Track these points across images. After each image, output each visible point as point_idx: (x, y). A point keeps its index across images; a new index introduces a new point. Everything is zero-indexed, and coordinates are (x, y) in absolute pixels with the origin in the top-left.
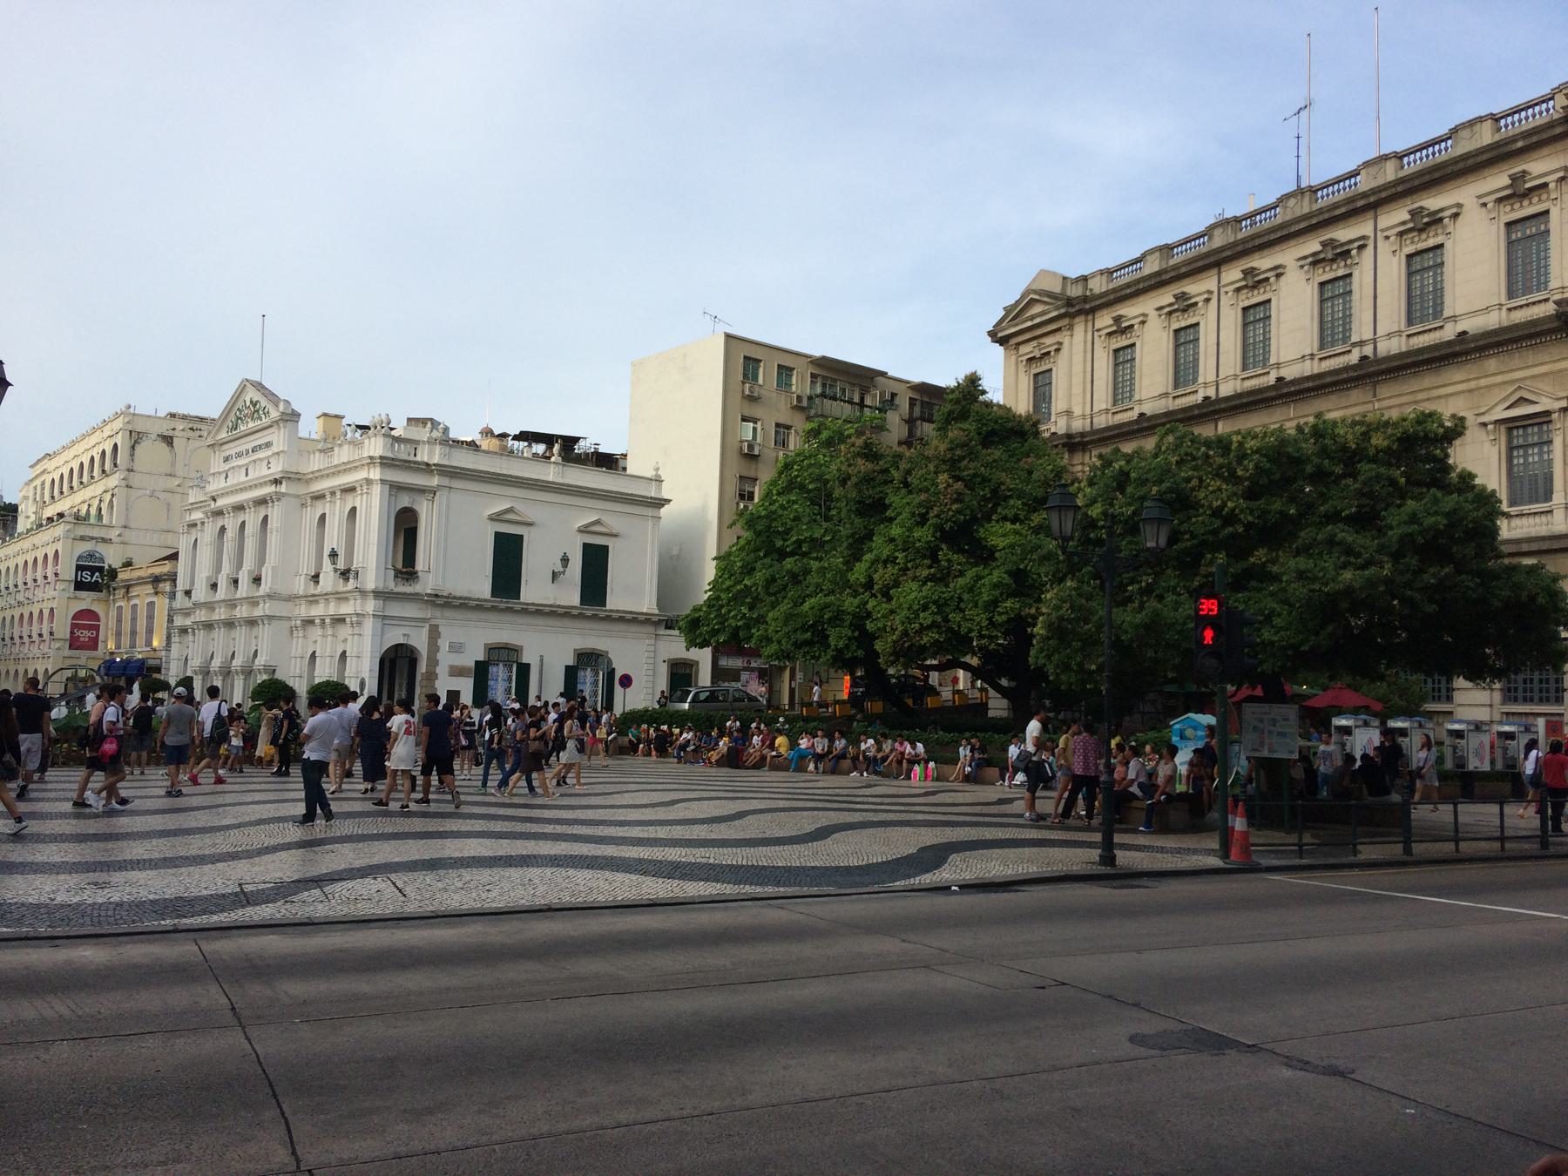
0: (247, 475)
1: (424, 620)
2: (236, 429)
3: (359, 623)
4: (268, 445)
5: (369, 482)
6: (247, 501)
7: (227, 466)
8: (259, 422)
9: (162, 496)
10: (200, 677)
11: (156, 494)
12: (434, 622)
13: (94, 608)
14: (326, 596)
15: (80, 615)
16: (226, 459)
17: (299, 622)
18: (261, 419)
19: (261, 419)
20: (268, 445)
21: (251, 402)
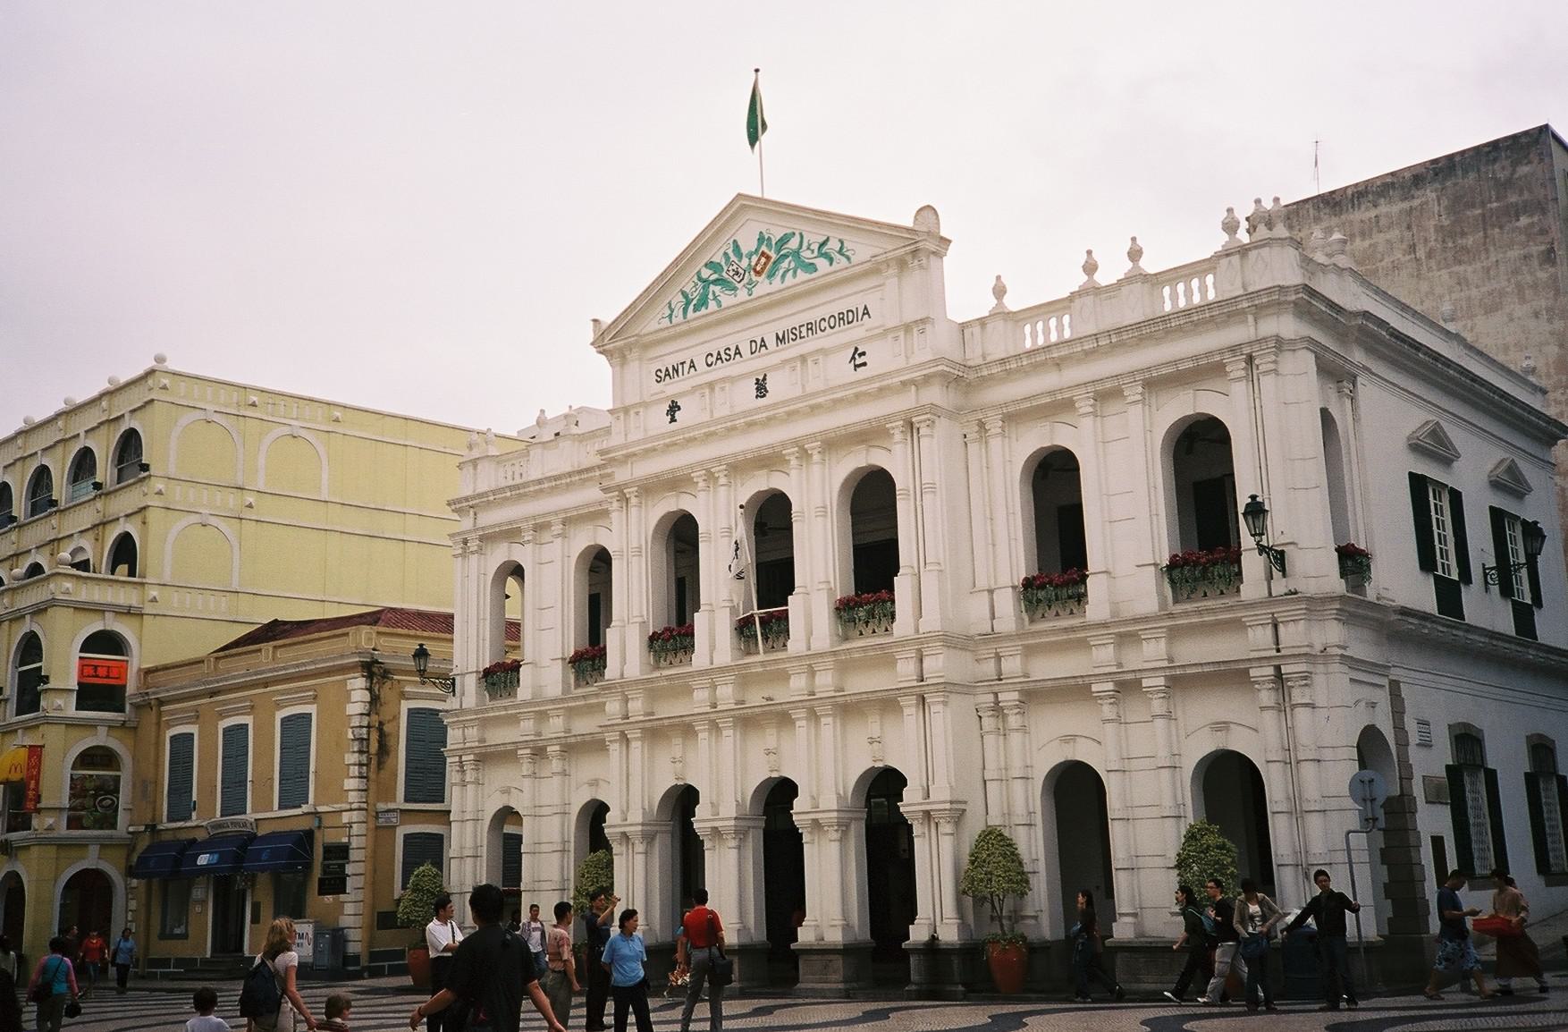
0: (761, 389)
1: (1373, 668)
2: (703, 302)
3: (1306, 676)
4: (844, 318)
5: (1280, 344)
6: (796, 442)
7: (672, 388)
8: (802, 276)
9: (223, 525)
10: (640, 848)
11: (213, 520)
12: (1395, 674)
13: (113, 744)
14: (1126, 633)
15: (90, 758)
16: (665, 375)
17: (1009, 697)
18: (812, 267)
19: (812, 267)
20: (844, 318)
21: (761, 239)
